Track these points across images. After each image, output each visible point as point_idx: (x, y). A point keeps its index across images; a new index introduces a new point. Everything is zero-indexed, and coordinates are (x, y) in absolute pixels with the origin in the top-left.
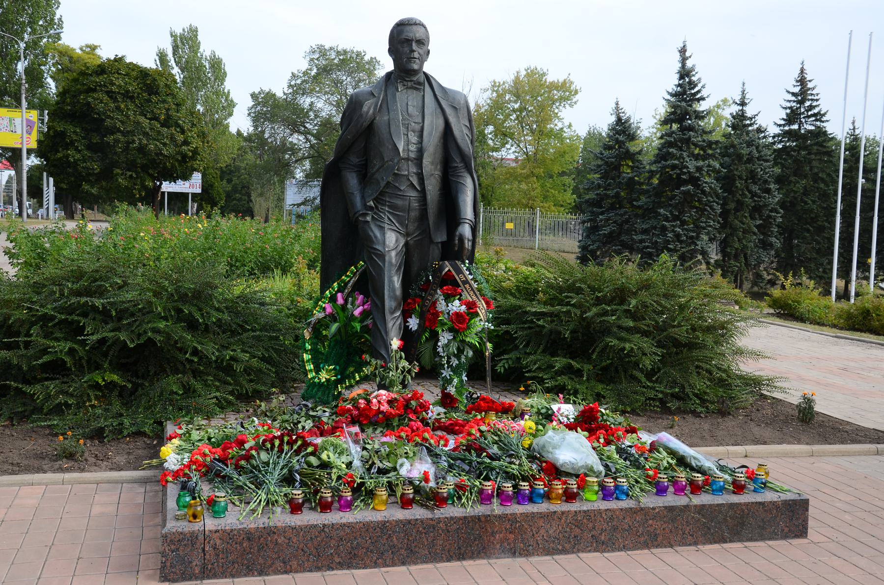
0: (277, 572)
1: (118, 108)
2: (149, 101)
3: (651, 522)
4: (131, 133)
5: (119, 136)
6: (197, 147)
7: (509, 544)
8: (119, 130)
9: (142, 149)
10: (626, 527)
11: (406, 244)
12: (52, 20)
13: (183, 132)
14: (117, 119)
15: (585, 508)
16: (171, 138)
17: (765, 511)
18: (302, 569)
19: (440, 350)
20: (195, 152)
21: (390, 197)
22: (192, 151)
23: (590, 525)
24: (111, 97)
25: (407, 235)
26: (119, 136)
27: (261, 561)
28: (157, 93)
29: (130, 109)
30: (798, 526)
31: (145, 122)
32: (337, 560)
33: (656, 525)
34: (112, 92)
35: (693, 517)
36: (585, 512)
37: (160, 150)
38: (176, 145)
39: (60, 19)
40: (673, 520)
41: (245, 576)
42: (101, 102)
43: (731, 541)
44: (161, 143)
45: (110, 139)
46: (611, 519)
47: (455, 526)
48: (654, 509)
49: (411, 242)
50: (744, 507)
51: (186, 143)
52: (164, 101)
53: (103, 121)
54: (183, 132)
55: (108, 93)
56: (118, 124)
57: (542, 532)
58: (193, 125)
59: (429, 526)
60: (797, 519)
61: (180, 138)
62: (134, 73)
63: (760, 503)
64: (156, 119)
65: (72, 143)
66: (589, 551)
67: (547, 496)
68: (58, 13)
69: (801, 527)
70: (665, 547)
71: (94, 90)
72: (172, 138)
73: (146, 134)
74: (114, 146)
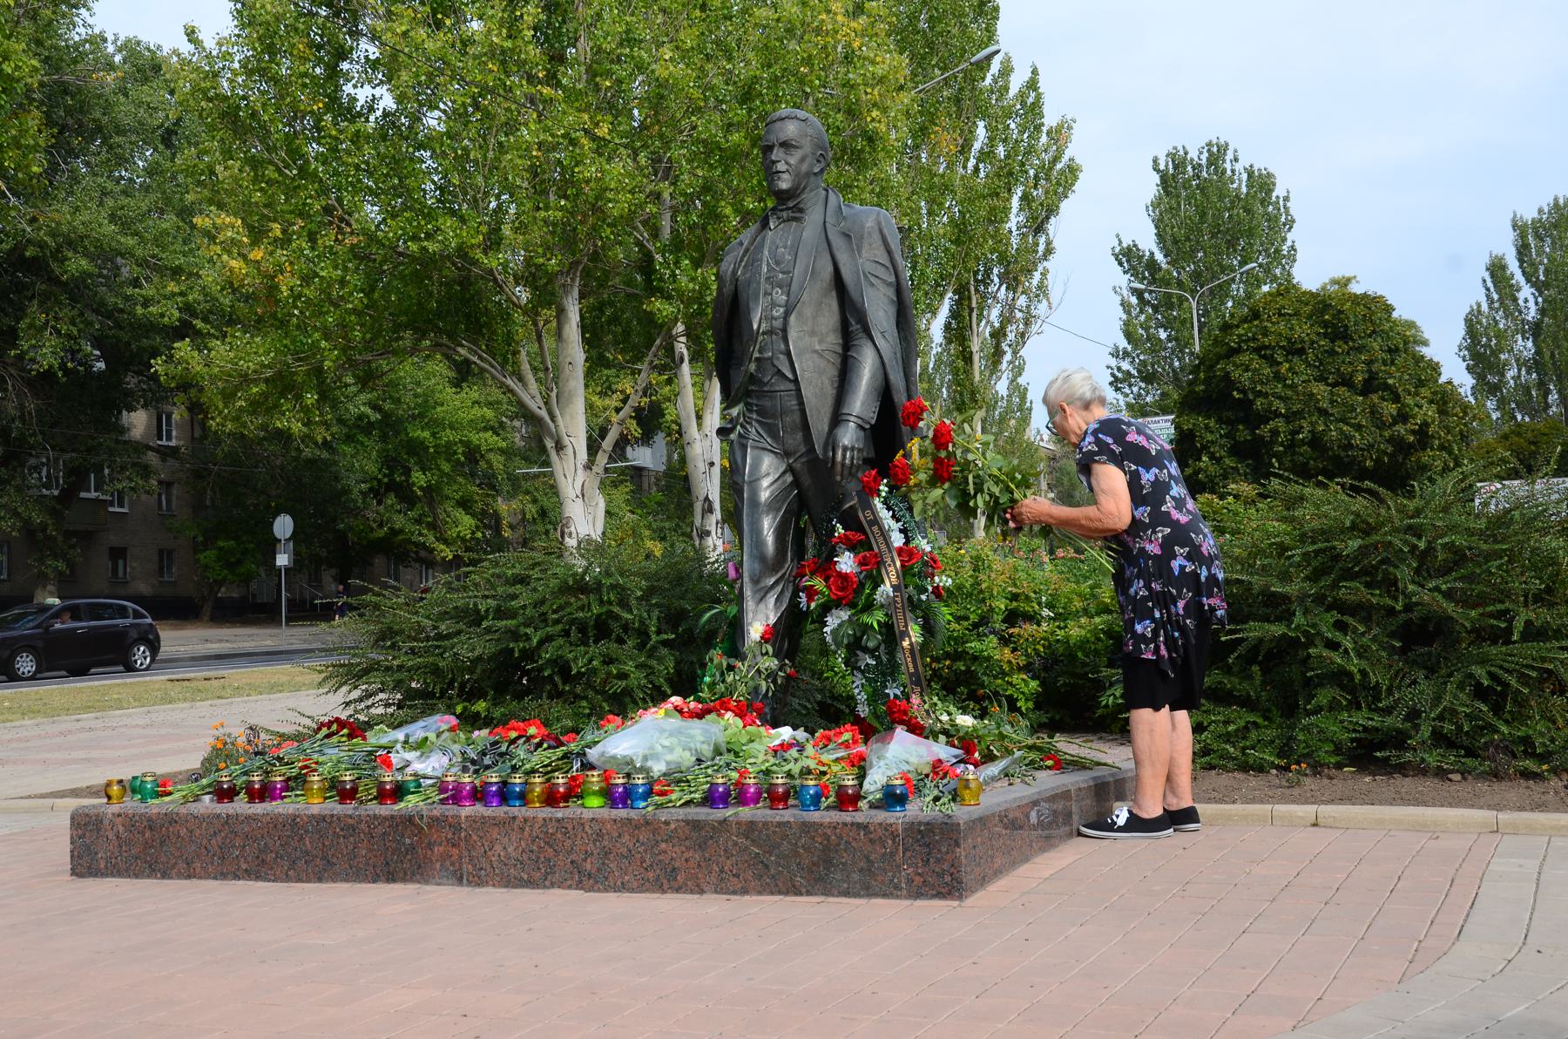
0: (180, 876)
1: (1278, 377)
2: (1332, 353)
3: (663, 845)
4: (1298, 415)
5: (1279, 424)
6: (1425, 424)
7: (452, 864)
8: (1277, 414)
9: (1316, 441)
10: (624, 851)
11: (790, 469)
12: (1277, 251)
13: (1396, 398)
14: (1273, 395)
15: (560, 815)
16: (1372, 413)
17: (871, 840)
18: (207, 876)
19: (829, 639)
20: (1422, 433)
21: (758, 398)
22: (1413, 432)
23: (568, 843)
24: (1264, 357)
25: (786, 454)
26: (1279, 424)
27: (164, 859)
28: (1345, 336)
29: (1300, 373)
30: (941, 875)
31: (1320, 389)
32: (244, 866)
33: (672, 851)
34: (1266, 347)
35: (736, 844)
36: (558, 820)
37: (1349, 438)
38: (1381, 426)
39: (1293, 248)
40: (702, 846)
41: (149, 877)
42: (1245, 371)
43: (809, 893)
44: (1352, 425)
45: (1264, 431)
46: (600, 835)
47: (380, 830)
48: (667, 823)
49: (798, 466)
50: (829, 832)
51: (1403, 417)
52: (1360, 349)
53: (1251, 402)
54: (1396, 398)
55: (1257, 350)
56: (1277, 404)
57: (498, 848)
58: (1421, 383)
59: (350, 827)
60: (938, 861)
61: (1390, 409)
62: (1308, 309)
63: (859, 826)
64: (1347, 382)
65: (1205, 447)
66: (570, 887)
67: (523, 797)
68: (1289, 236)
69: (948, 878)
70: (692, 892)
71: (1238, 351)
72: (1374, 412)
73: (1323, 412)
74: (1273, 442)
